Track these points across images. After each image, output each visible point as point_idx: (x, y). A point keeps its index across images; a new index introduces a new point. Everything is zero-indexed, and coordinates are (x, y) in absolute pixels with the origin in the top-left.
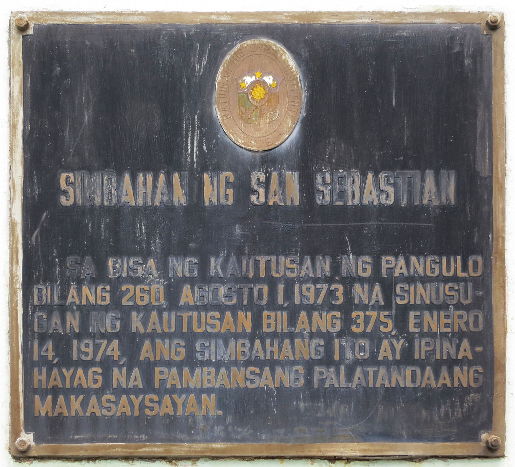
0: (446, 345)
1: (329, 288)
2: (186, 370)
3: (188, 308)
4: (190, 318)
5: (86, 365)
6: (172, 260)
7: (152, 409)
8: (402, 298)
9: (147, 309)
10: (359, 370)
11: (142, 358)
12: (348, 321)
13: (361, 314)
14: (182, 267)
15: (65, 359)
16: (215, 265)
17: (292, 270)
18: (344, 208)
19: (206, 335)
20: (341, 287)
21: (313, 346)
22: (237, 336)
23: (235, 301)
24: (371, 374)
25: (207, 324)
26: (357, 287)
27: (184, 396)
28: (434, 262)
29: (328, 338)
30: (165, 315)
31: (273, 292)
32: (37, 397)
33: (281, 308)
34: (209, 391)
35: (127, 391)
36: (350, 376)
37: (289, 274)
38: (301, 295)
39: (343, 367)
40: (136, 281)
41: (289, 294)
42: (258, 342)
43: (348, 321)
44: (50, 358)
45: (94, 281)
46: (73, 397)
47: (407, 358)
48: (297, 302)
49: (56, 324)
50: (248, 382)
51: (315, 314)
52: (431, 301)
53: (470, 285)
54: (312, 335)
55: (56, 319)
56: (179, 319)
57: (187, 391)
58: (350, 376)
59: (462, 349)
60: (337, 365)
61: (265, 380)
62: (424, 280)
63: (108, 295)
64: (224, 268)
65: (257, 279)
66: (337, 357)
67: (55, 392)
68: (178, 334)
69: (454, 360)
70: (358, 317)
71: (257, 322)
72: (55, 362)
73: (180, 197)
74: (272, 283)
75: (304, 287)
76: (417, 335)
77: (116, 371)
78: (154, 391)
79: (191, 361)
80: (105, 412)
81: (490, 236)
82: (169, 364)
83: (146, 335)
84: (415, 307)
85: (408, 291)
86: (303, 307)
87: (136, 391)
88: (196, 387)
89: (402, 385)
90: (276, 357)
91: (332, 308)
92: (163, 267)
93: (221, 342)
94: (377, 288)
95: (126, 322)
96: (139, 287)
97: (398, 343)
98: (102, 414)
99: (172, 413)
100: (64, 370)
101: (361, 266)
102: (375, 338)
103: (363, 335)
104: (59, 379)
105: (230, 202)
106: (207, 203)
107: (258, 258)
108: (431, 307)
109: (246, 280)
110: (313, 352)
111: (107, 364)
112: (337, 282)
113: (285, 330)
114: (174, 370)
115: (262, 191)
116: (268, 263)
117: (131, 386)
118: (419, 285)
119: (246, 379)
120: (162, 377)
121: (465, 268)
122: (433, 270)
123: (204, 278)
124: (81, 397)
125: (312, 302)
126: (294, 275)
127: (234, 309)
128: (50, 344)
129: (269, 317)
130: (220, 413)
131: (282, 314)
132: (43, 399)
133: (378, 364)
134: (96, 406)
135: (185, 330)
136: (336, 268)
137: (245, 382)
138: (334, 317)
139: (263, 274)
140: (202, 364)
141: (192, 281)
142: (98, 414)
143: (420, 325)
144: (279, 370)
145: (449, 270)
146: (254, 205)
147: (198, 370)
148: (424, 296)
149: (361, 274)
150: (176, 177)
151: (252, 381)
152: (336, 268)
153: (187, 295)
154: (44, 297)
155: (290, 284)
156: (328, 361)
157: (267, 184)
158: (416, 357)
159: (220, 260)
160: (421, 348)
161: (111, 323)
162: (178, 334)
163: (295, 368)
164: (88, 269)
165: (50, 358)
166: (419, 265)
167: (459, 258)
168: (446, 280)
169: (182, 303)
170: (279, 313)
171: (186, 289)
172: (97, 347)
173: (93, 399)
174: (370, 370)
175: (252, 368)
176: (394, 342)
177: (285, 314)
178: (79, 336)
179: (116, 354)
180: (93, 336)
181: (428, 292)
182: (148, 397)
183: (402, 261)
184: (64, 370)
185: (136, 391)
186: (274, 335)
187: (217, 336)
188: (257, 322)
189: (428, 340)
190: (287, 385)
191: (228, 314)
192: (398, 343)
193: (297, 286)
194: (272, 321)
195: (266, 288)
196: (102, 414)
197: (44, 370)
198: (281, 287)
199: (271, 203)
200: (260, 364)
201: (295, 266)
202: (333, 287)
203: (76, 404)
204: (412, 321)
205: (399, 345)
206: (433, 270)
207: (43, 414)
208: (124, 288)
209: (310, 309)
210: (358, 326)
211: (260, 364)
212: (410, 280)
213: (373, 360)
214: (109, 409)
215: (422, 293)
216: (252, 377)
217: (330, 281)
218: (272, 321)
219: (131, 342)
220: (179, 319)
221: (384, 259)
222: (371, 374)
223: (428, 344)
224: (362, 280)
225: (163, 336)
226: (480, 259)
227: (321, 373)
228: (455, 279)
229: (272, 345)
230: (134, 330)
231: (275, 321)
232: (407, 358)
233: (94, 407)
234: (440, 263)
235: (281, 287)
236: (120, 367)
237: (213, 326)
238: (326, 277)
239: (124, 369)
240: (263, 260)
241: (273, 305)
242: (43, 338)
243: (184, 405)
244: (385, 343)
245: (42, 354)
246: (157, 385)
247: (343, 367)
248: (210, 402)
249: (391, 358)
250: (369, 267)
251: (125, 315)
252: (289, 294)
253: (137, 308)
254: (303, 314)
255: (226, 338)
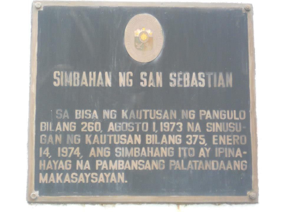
0: (230, 150)
1: (176, 125)
2: (111, 162)
3: (111, 132)
4: (113, 138)
5: (64, 159)
6: (105, 111)
7: (94, 180)
8: (209, 129)
9: (94, 133)
10: (190, 162)
11: (90, 156)
12: (184, 139)
13: (191, 136)
14: (107, 114)
15: (54, 156)
16: (124, 114)
17: (159, 116)
18: (183, 88)
19: (120, 145)
20: (181, 124)
21: (169, 150)
22: (134, 146)
23: (133, 130)
24: (196, 164)
25: (120, 140)
26: (189, 124)
27: (109, 174)
28: (223, 113)
29: (176, 147)
30: (101, 136)
31: (150, 126)
32: (41, 174)
33: (154, 133)
34: (121, 171)
35: (84, 171)
36: (186, 165)
37: (158, 118)
38: (164, 128)
39: (182, 161)
40: (87, 121)
41: (158, 127)
42: (143, 149)
43: (184, 139)
44: (47, 156)
45: (67, 120)
46: (58, 174)
47: (212, 156)
48: (162, 130)
49: (50, 140)
50: (139, 168)
51: (170, 136)
52: (222, 131)
53: (240, 124)
54: (168, 146)
55: (51, 137)
56: (108, 138)
57: (111, 171)
58: (186, 165)
59: (237, 152)
60: (180, 159)
61: (148, 166)
62: (219, 121)
63: (75, 127)
64: (128, 114)
65: (143, 120)
66: (180, 155)
67: (49, 172)
68: (107, 145)
69: (234, 158)
70: (189, 137)
71: (143, 139)
72: (50, 157)
73: (109, 82)
74: (150, 121)
75: (165, 124)
76: (216, 146)
77: (78, 162)
78: (95, 171)
79: (113, 158)
80: (73, 181)
81: (249, 101)
82: (103, 159)
83: (92, 145)
84: (215, 133)
85: (212, 126)
86: (164, 133)
87: (87, 171)
88: (115, 169)
89: (210, 169)
90: (152, 156)
91: (179, 133)
92: (100, 114)
93: (126, 148)
94: (198, 124)
95: (83, 139)
96: (89, 123)
97: (208, 149)
98: (71, 182)
99: (104, 181)
100: (54, 161)
101: (191, 114)
102: (197, 147)
103: (192, 146)
104: (51, 165)
105: (131, 85)
106: (121, 85)
107: (144, 110)
108: (222, 134)
109: (137, 120)
110: (169, 154)
111: (74, 158)
112: (179, 121)
113: (156, 143)
114: (105, 162)
115: (145, 80)
116: (148, 113)
117: (85, 169)
118: (217, 124)
119: (138, 166)
120: (100, 165)
121: (237, 116)
122: (223, 117)
123: (119, 119)
124: (62, 174)
125: (168, 130)
126: (160, 118)
127: (133, 134)
128: (47, 149)
129: (149, 137)
130: (126, 182)
131: (155, 136)
132: (44, 176)
133: (199, 159)
134: (69, 178)
135: (110, 143)
136: (179, 115)
137: (138, 167)
138: (178, 137)
139: (146, 118)
140: (118, 159)
141: (114, 121)
142: (69, 182)
143: (218, 141)
144: (153, 162)
145: (230, 116)
146: (142, 87)
147: (116, 161)
148: (219, 129)
149: (190, 118)
150: (106, 73)
151: (141, 167)
152: (179, 115)
153: (111, 127)
154: (45, 128)
155: (158, 122)
156: (176, 157)
157: (147, 78)
158: (216, 156)
159: (127, 111)
160: (218, 152)
161: (76, 139)
162: (107, 145)
163: (161, 161)
164: (66, 115)
165: (47, 156)
166: (216, 114)
167: (235, 111)
168: (229, 121)
169: (109, 130)
170: (153, 135)
171: (111, 124)
172: (69, 151)
173: (67, 175)
174: (195, 162)
175: (140, 161)
176: (206, 149)
177: (156, 136)
178: (61, 146)
179: (78, 154)
180: (68, 146)
181: (221, 127)
182: (93, 174)
183: (209, 112)
184: (54, 161)
185: (87, 171)
186: (151, 145)
187: (125, 146)
188: (143, 139)
189: (221, 148)
190: (157, 168)
191: (130, 136)
192: (208, 149)
193: (161, 123)
194: (150, 139)
195: (147, 124)
196: (71, 182)
197: (44, 161)
198: (154, 124)
199: (149, 86)
200: (145, 159)
201: (160, 114)
202: (178, 124)
203: (59, 177)
204: (214, 140)
205: (208, 150)
206: (223, 117)
207: (43, 182)
208: (82, 123)
209: (167, 134)
210: (189, 141)
211: (145, 159)
212: (215, 120)
213: (196, 157)
214: (74, 180)
215: (217, 127)
216: (141, 165)
217: (176, 121)
218: (150, 139)
219: (85, 149)
220: (108, 138)
221: (201, 111)
222: (196, 164)
223: (221, 150)
224: (191, 121)
225: (100, 146)
226: (244, 112)
227: (173, 163)
228: (233, 121)
229: (150, 150)
230: (87, 143)
231: (151, 139)
232: (212, 156)
233: (67, 179)
234: (226, 113)
235: (154, 124)
236: (80, 160)
237: (123, 141)
238: (174, 119)
239: (82, 161)
240: (146, 111)
241: (150, 132)
242: (44, 147)
243: (110, 178)
244: (202, 150)
245: (44, 154)
246: (97, 168)
247: (182, 161)
248: (121, 177)
249: (204, 156)
250: (194, 115)
251: (83, 135)
252: (158, 127)
253: (88, 133)
254: (164, 137)
255: (130, 146)
